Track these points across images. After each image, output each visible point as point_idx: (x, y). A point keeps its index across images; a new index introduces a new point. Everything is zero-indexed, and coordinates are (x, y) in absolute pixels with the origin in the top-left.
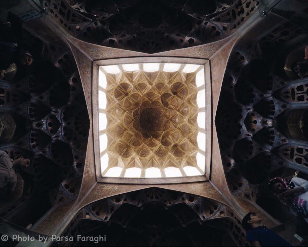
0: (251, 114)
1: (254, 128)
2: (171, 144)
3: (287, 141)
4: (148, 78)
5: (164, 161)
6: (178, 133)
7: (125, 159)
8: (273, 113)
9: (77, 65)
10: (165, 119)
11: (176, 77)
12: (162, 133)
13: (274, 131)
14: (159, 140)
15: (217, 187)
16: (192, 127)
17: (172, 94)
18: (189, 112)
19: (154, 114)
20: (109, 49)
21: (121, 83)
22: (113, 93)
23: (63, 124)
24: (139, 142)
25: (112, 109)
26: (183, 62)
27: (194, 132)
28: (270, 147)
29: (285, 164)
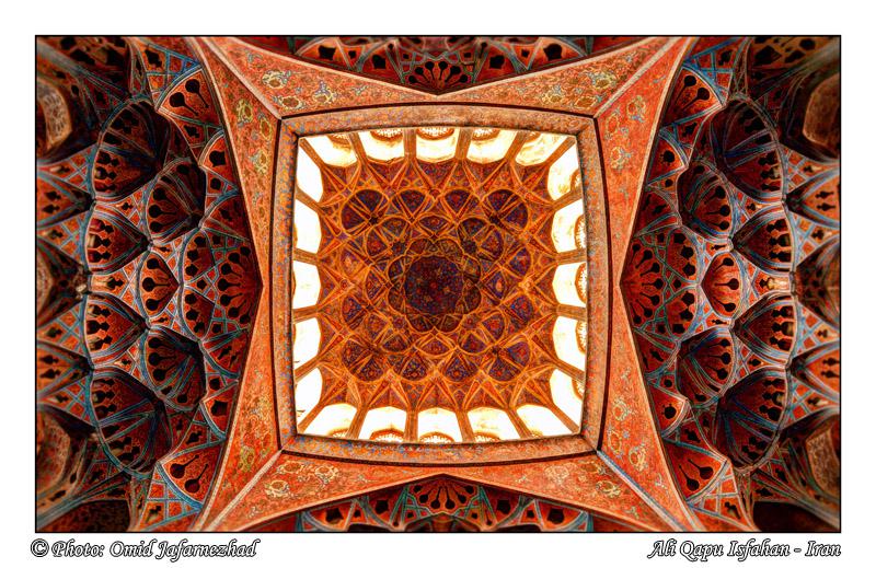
0: (722, 261)
2: (482, 346)
4: (429, 179)
5: (466, 390)
6: (501, 318)
7: (366, 383)
8: (786, 257)
9: (224, 113)
10: (467, 285)
11: (497, 174)
12: (461, 318)
14: (453, 337)
15: (627, 474)
16: (538, 303)
17: (488, 222)
18: (532, 266)
19: (439, 272)
20: (320, 73)
21: (359, 189)
22: (340, 217)
23: (185, 285)
24: (401, 341)
25: (335, 254)
26: (525, 125)
27: (544, 315)
28: (785, 356)
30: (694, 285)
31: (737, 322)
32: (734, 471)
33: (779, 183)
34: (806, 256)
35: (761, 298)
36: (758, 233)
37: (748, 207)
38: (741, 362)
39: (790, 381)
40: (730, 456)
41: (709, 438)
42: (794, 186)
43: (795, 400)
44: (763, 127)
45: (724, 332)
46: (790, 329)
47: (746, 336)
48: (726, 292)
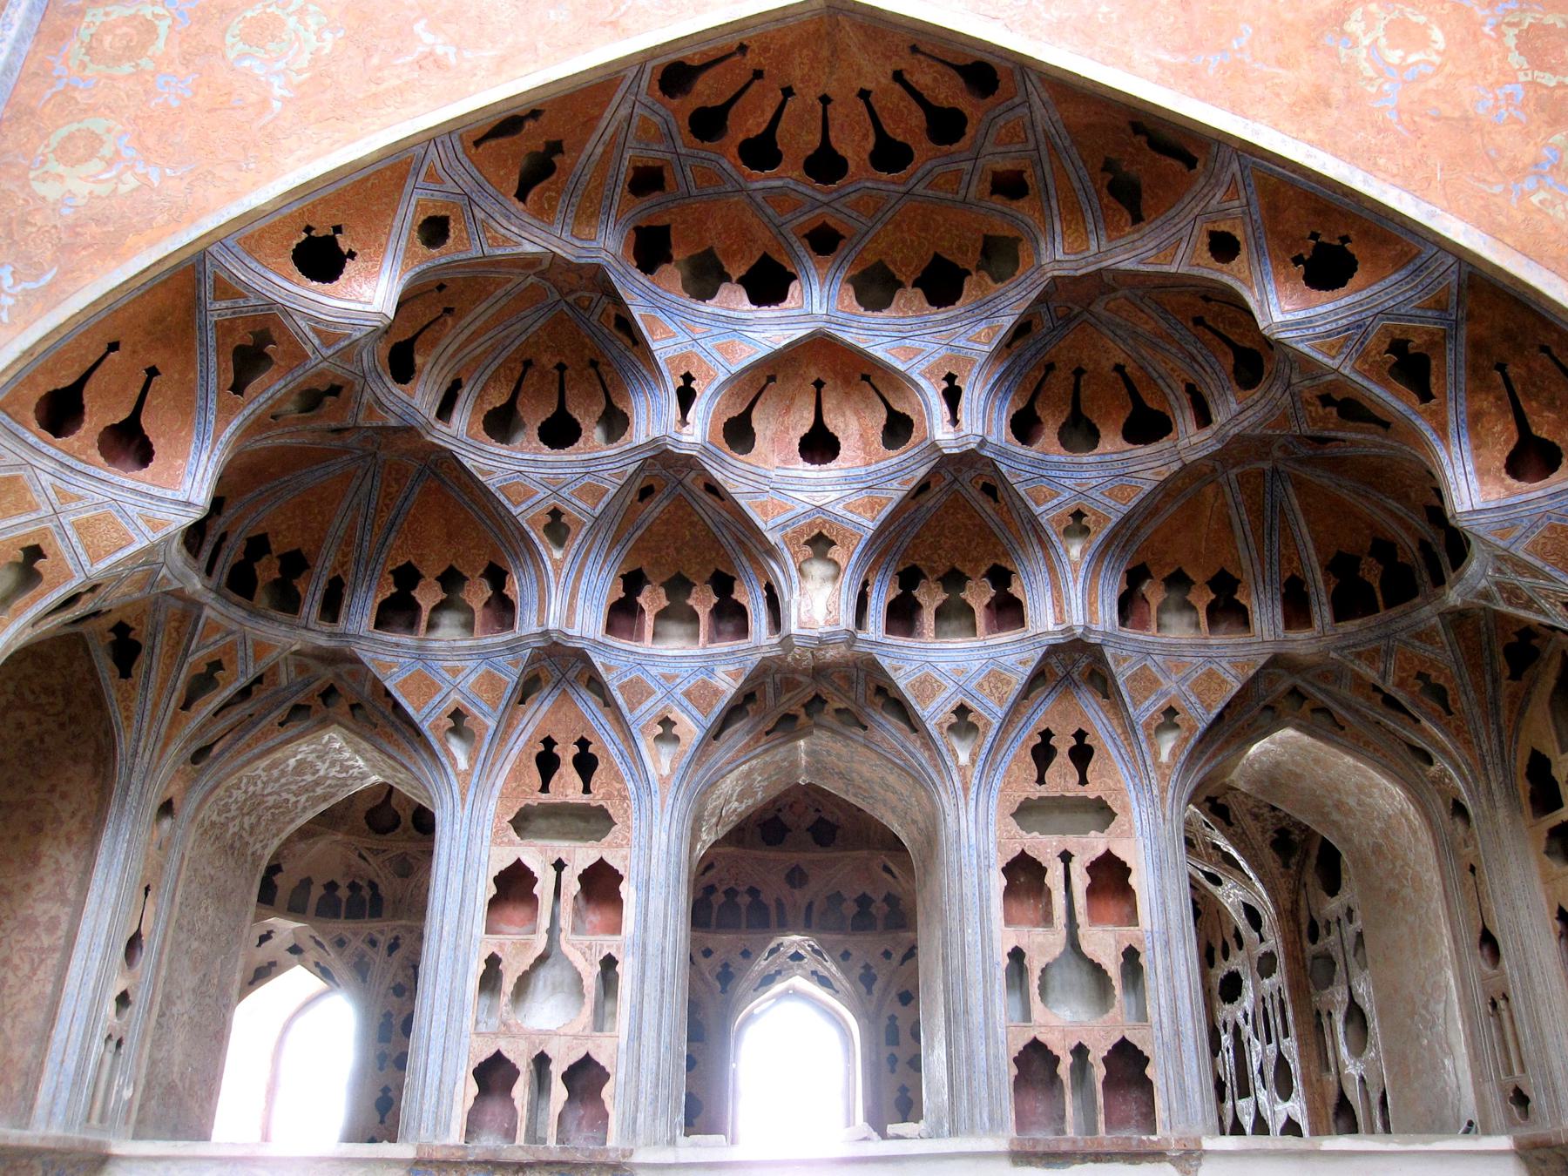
1: (760, 443)
3: (661, 762)
8: (902, 616)
13: (741, 644)
29: (463, 763)
30: (816, 304)
31: (689, 462)
32: (167, 540)
33: (1142, 625)
34: (901, 684)
35: (773, 538)
36: (986, 534)
37: (1078, 515)
38: (554, 485)
39: (512, 648)
40: (217, 504)
41: (257, 426)
42: (1122, 674)
43: (455, 672)
44: (1342, 613)
45: (652, 419)
46: (673, 628)
47: (646, 493)
48: (791, 419)
